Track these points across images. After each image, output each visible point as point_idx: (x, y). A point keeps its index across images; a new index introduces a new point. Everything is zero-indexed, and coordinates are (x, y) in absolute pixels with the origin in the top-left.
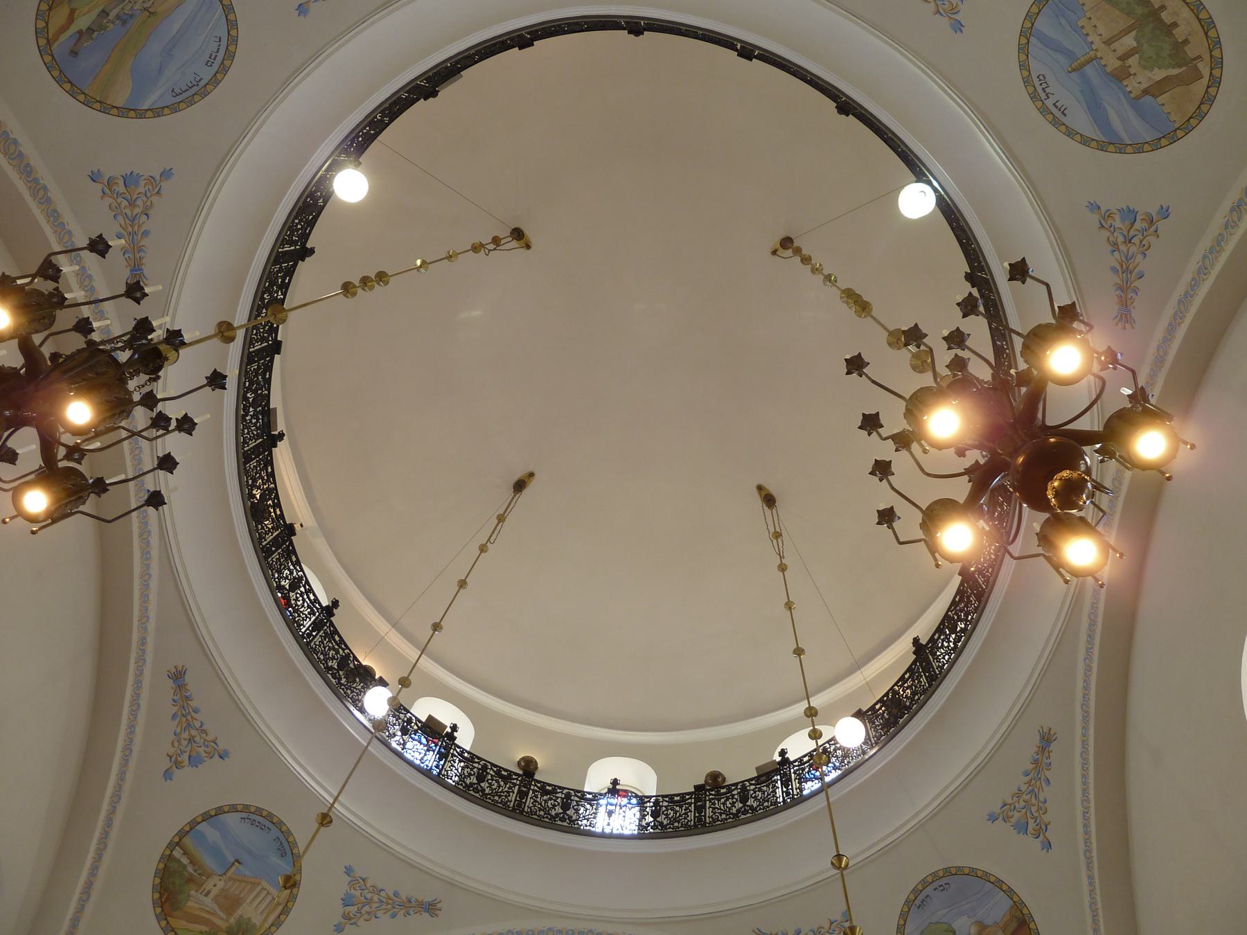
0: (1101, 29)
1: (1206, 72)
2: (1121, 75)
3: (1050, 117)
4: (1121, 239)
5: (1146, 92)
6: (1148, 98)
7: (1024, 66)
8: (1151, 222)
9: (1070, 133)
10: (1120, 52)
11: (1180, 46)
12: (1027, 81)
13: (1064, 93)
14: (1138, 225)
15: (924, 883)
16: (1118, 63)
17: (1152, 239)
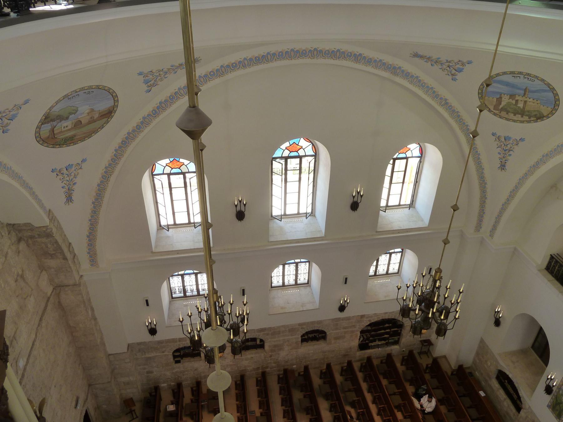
0: (531, 103)
1: (494, 111)
2: (512, 96)
3: (516, 73)
4: (451, 64)
5: (501, 98)
6: (498, 96)
7: (543, 80)
8: (453, 75)
9: (505, 73)
10: (519, 102)
11: (508, 112)
12: (537, 77)
13: (521, 81)
14: (454, 71)
15: (82, 89)
16: (516, 99)
17: (446, 72)
